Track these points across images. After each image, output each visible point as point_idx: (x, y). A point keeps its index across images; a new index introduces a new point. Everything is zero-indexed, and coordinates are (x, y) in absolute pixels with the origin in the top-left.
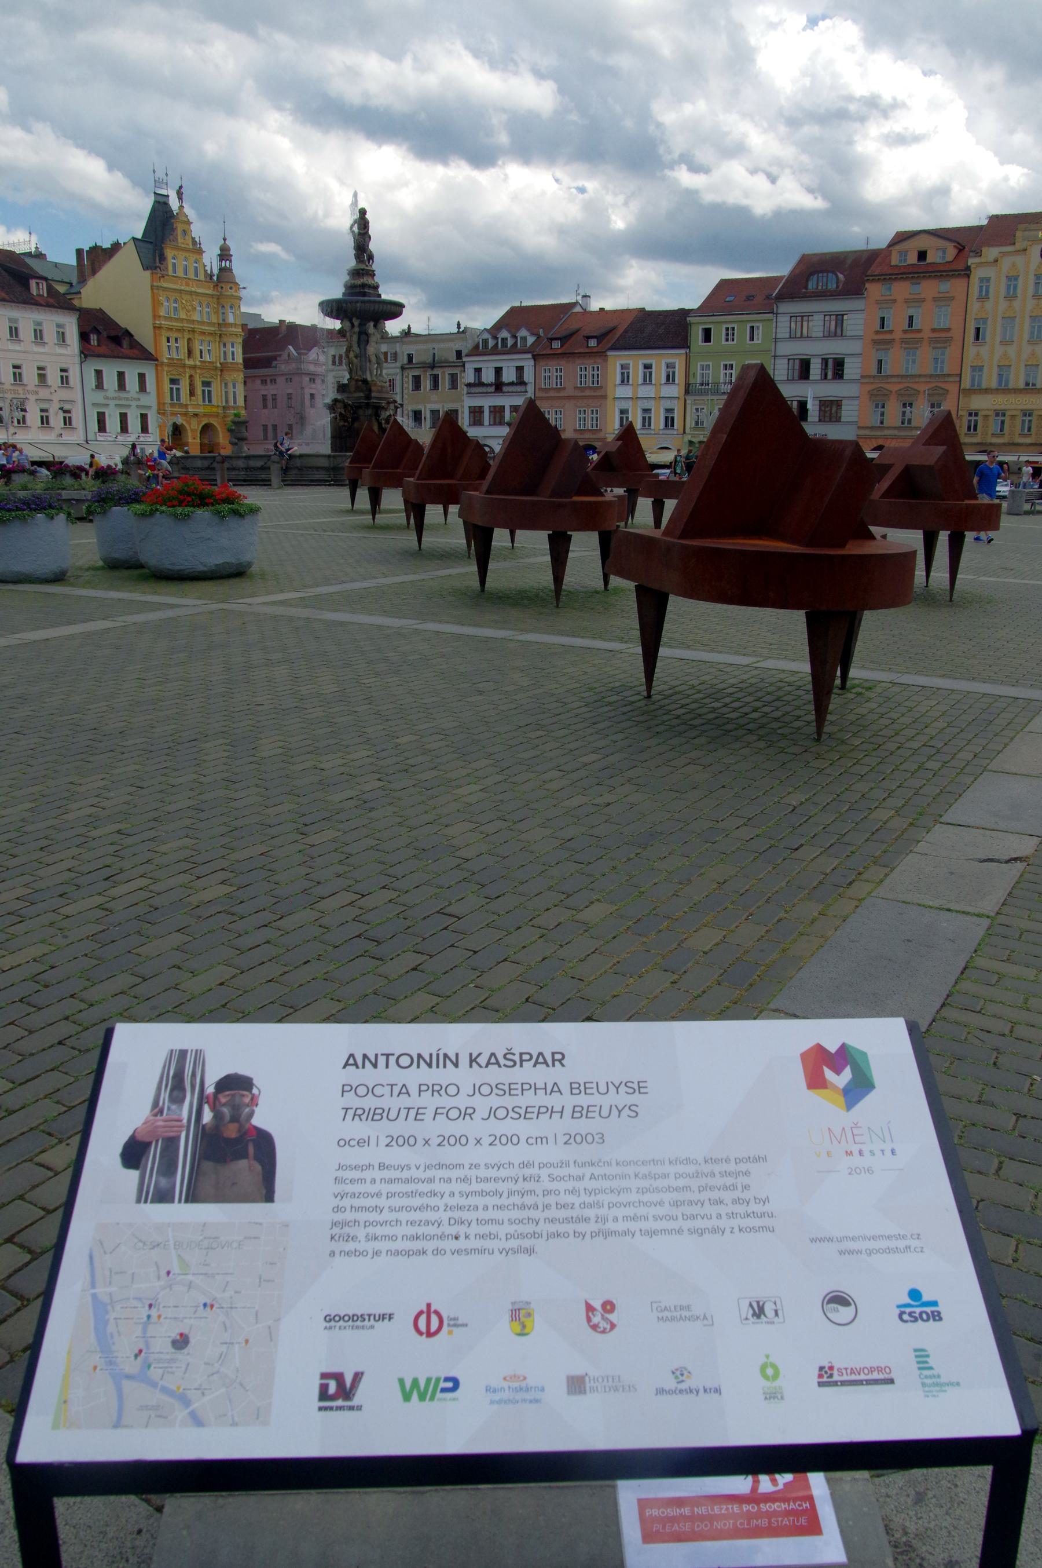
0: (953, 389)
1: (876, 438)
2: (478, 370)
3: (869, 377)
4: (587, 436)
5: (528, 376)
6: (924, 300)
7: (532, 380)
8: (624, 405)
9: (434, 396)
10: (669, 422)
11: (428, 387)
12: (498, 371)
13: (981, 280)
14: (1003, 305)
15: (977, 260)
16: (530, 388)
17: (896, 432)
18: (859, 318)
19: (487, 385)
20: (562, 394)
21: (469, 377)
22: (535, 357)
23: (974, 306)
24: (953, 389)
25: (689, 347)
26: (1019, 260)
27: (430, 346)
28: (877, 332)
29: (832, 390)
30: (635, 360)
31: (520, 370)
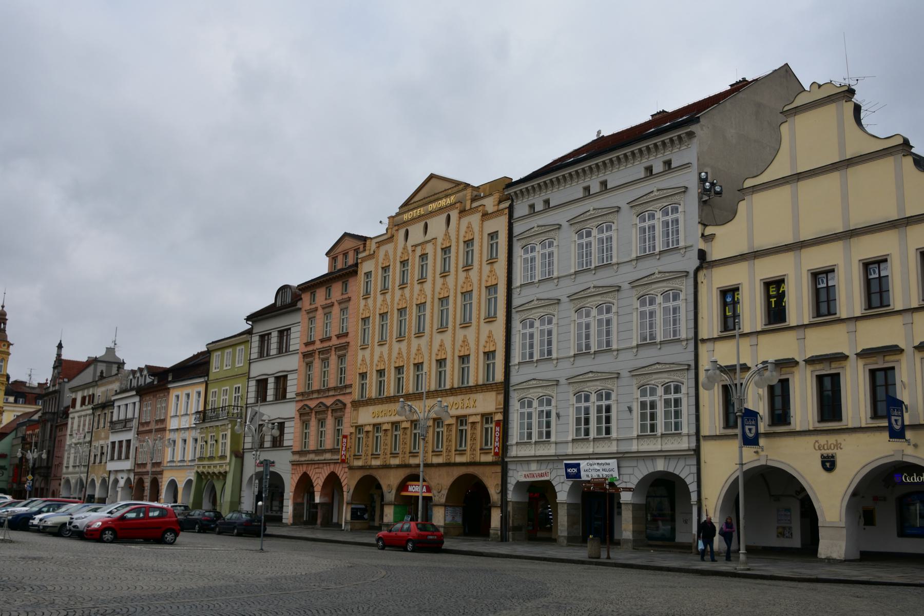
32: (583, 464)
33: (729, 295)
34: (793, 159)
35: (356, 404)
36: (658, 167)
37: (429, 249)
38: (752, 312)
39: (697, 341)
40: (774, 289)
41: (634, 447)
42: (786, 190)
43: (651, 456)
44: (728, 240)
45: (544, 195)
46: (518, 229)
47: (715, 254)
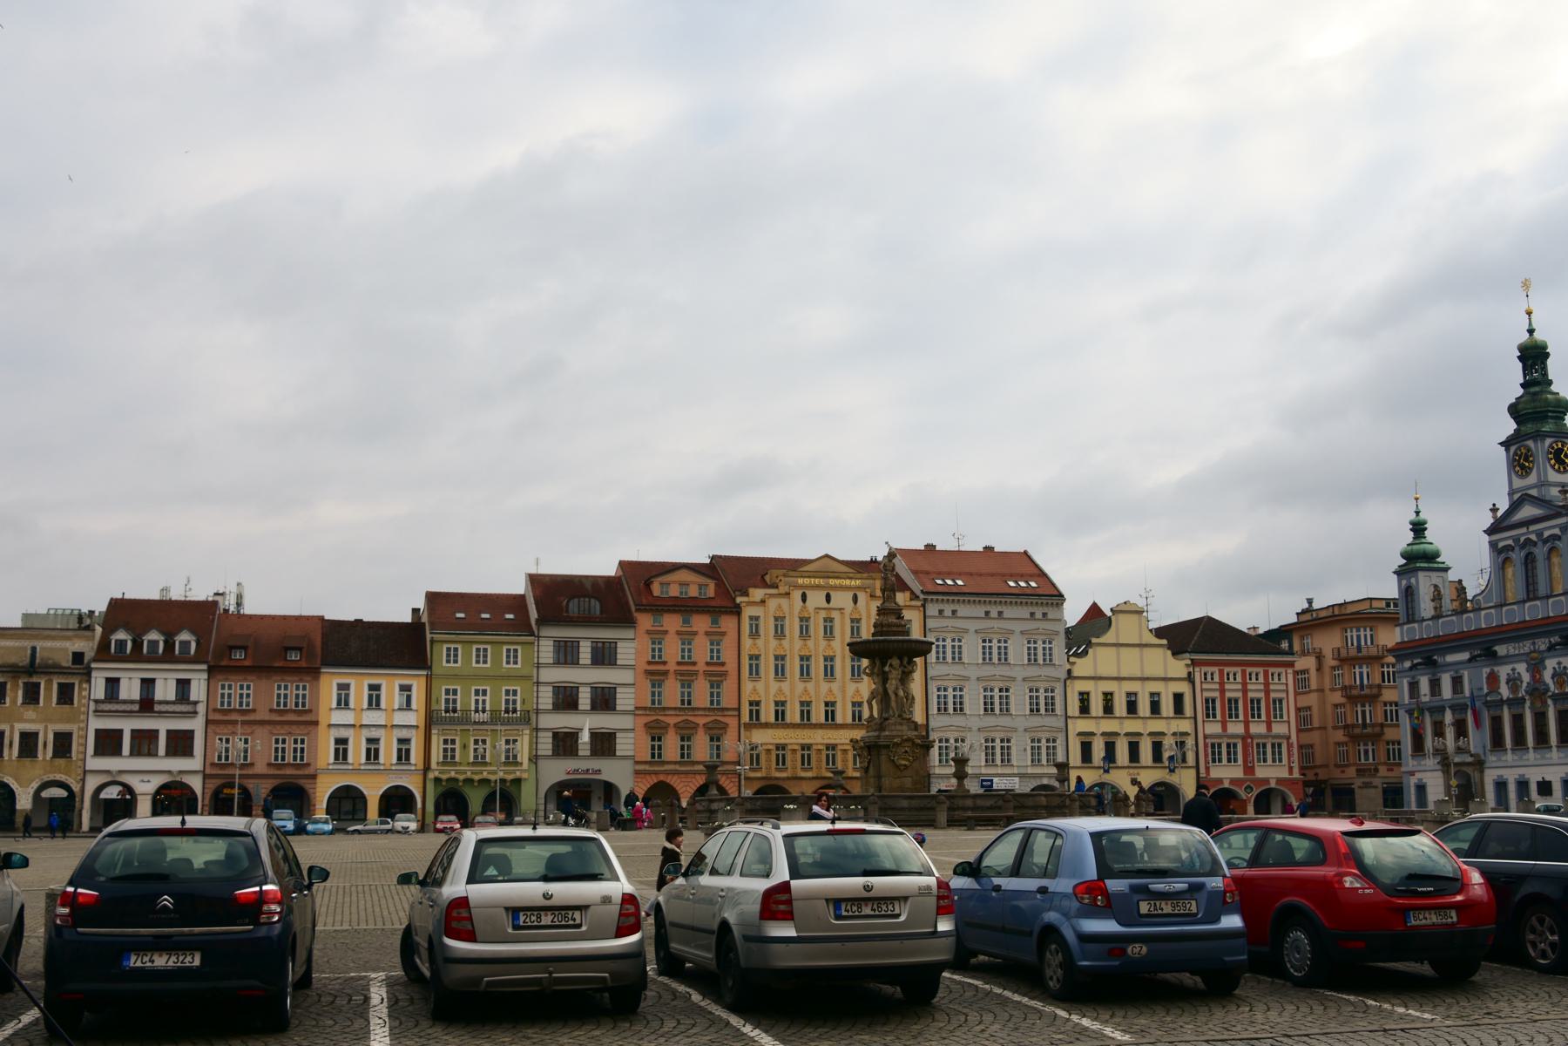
0: (732, 722)
1: (656, 773)
2: (113, 683)
3: (645, 708)
4: (289, 772)
5: (198, 690)
6: (695, 633)
7: (203, 697)
8: (343, 733)
9: (30, 713)
10: (404, 756)
11: (20, 700)
12: (148, 684)
13: (751, 618)
14: (798, 644)
15: (745, 599)
16: (201, 708)
17: (678, 767)
18: (630, 648)
19: (125, 702)
20: (251, 717)
21: (99, 689)
22: (212, 671)
23: (747, 643)
24: (732, 722)
25: (430, 668)
26: (784, 602)
27: (28, 644)
28: (649, 663)
29: (605, 721)
30: (359, 683)
31: (183, 685)
32: (996, 780)
33: (1084, 699)
34: (1117, 636)
35: (748, 727)
36: (1039, 615)
37: (835, 615)
38: (1096, 706)
39: (1067, 717)
40: (1108, 698)
41: (1030, 771)
42: (1114, 649)
43: (1041, 776)
44: (1082, 667)
45: (953, 607)
46: (931, 624)
47: (1076, 673)
